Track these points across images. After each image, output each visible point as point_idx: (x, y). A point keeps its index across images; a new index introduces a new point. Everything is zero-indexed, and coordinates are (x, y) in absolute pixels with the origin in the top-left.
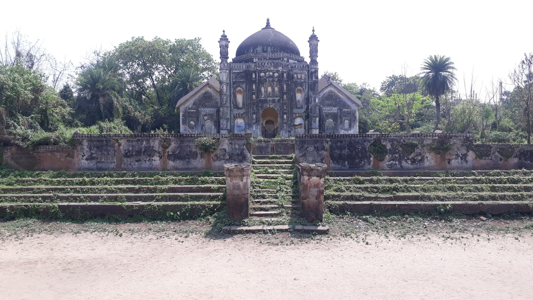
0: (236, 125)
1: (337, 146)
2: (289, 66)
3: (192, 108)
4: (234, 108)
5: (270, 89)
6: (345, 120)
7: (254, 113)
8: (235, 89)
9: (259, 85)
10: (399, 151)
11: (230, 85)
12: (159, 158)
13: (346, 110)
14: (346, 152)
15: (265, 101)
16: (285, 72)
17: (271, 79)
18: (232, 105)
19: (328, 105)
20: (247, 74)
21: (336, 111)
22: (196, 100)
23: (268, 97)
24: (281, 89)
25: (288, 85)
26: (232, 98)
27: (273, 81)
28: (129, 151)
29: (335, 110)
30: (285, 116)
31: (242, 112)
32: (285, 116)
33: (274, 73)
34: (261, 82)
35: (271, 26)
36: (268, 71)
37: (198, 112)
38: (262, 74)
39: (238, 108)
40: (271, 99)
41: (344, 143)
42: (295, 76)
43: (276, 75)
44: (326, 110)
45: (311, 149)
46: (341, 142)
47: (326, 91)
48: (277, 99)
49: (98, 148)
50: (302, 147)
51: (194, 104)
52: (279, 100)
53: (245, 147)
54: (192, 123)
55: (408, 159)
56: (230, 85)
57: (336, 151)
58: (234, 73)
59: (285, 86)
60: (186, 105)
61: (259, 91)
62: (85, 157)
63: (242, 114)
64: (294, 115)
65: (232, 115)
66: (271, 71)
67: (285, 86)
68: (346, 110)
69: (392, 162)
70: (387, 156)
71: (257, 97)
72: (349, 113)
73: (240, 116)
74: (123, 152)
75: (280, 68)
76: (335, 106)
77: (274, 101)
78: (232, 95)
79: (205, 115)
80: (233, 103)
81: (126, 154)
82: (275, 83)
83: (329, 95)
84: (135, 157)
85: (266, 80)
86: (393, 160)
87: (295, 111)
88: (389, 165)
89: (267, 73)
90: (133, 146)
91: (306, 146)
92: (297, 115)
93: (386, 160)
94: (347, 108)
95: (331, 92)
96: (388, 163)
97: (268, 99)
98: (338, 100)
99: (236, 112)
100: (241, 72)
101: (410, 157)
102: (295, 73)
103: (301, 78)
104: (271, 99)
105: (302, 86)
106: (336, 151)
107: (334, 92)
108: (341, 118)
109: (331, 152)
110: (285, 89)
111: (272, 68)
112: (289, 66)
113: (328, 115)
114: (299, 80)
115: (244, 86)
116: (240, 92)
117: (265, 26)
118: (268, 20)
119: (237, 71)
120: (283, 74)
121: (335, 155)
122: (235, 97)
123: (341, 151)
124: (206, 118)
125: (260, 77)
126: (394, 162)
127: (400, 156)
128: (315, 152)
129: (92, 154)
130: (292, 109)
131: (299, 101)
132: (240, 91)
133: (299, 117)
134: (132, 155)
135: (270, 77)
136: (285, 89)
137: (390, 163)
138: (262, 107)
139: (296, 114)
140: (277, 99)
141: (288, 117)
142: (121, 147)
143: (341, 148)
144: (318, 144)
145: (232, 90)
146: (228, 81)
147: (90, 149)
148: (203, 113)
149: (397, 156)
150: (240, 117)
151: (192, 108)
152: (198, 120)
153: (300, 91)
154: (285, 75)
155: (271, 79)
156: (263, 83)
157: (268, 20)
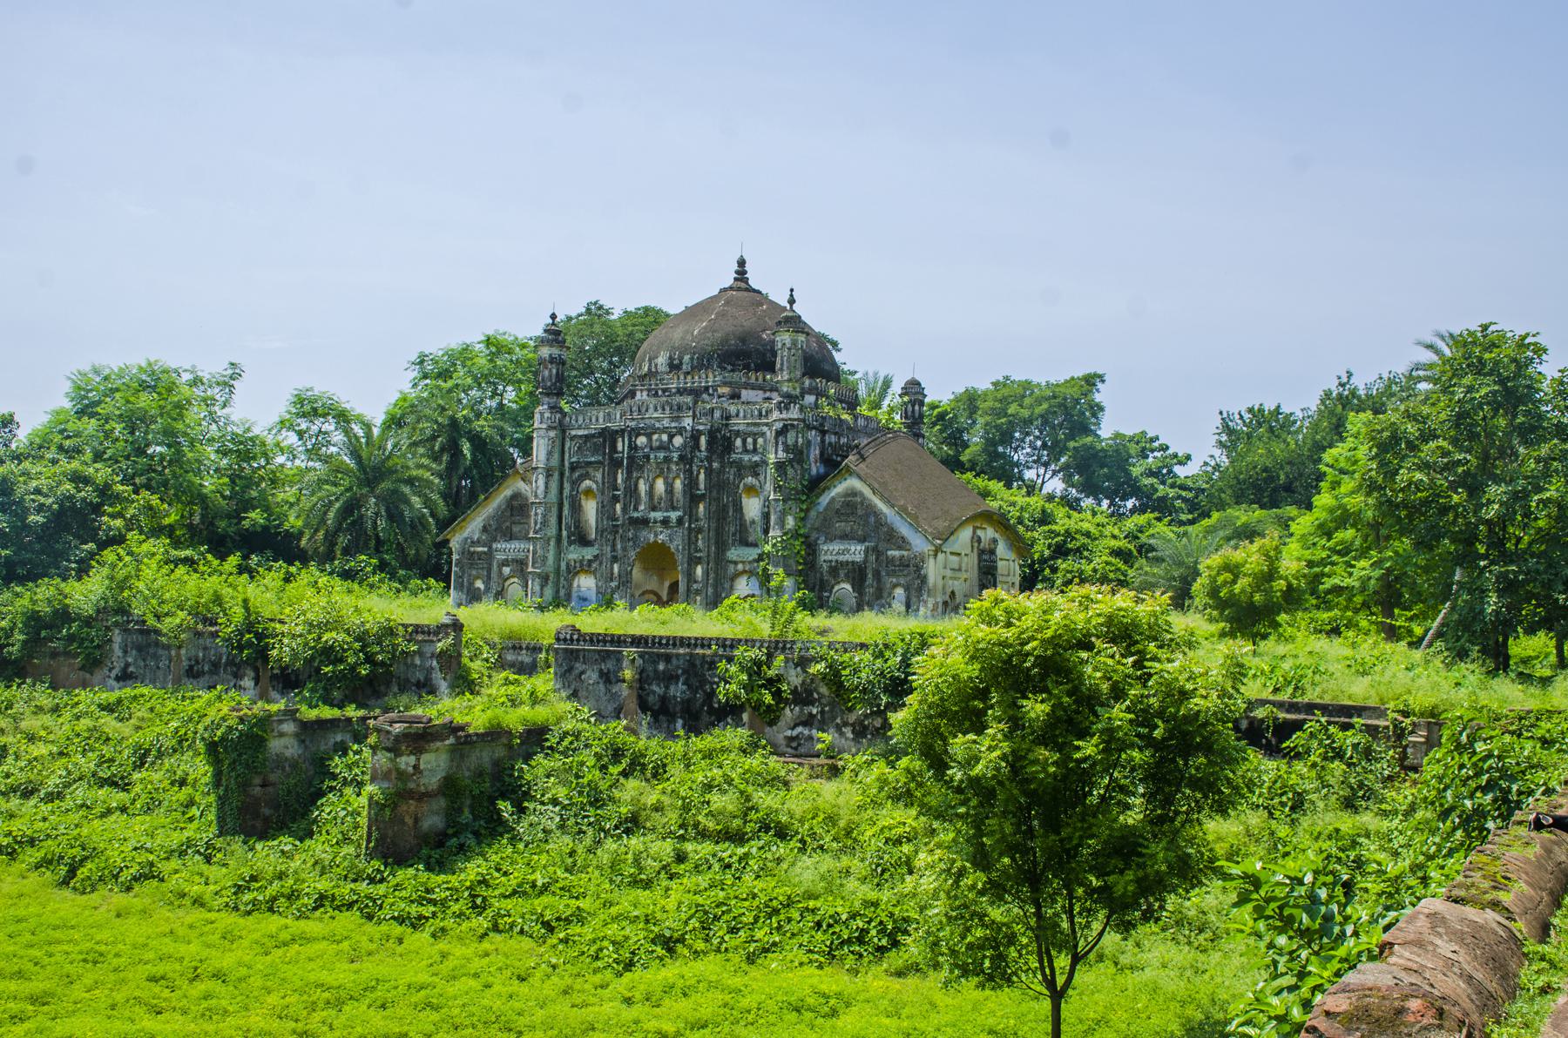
0: (574, 595)
1: (656, 671)
2: (717, 414)
3: (478, 543)
4: (570, 543)
5: (660, 485)
6: (895, 586)
7: (615, 559)
8: (575, 483)
9: (629, 472)
10: (821, 696)
11: (562, 475)
12: (252, 683)
13: (896, 553)
14: (678, 690)
15: (645, 522)
16: (700, 433)
17: (661, 455)
18: (564, 533)
19: (844, 537)
20: (609, 436)
21: (859, 558)
22: (489, 518)
23: (654, 509)
24: (691, 483)
25: (709, 472)
26: (566, 512)
27: (667, 460)
28: (197, 662)
29: (856, 552)
30: (699, 570)
31: (588, 553)
32: (699, 570)
33: (671, 437)
34: (636, 463)
35: (753, 283)
36: (656, 431)
37: (489, 555)
38: (642, 440)
39: (584, 541)
40: (658, 515)
41: (674, 661)
42: (738, 442)
43: (678, 441)
44: (831, 551)
45: (592, 676)
46: (668, 658)
47: (839, 488)
48: (674, 515)
49: (140, 649)
50: (570, 670)
51: (485, 529)
52: (680, 521)
53: (435, 663)
54: (479, 584)
55: (845, 724)
56: (562, 475)
57: (655, 688)
58: (572, 438)
59: (702, 476)
60: (465, 535)
61: (632, 491)
62: (113, 674)
63: (590, 561)
64: (731, 568)
65: (563, 565)
66: (664, 430)
67: (702, 476)
68: (896, 553)
69: (800, 729)
70: (787, 711)
71: (624, 510)
72: (904, 564)
73: (585, 567)
74: (185, 663)
75: (687, 422)
76: (862, 540)
77: (665, 522)
78: (566, 503)
79: (505, 563)
80: (568, 528)
81: (191, 667)
82: (674, 467)
83: (847, 504)
84: (207, 677)
85: (647, 457)
86: (804, 724)
87: (733, 554)
88: (791, 739)
89: (655, 437)
90: (205, 649)
91: (579, 666)
92: (740, 567)
93: (781, 723)
94: (900, 548)
95: (853, 493)
96: (789, 733)
97: (653, 515)
98: (872, 519)
99: (574, 554)
100: (593, 436)
101: (852, 718)
102: (738, 433)
103: (755, 450)
104: (658, 515)
105: (756, 475)
106: (655, 688)
107: (862, 494)
108: (877, 574)
109: (641, 688)
110: (702, 486)
111: (666, 423)
112: (717, 414)
113: (835, 569)
114: (746, 458)
115: (599, 476)
116: (588, 492)
117: (728, 280)
118: (742, 263)
119: (580, 433)
120: (695, 436)
121: (651, 699)
122: (576, 508)
123: (667, 688)
124: (506, 570)
125: (633, 447)
126: (806, 732)
127: (822, 712)
128: (601, 686)
129: (127, 665)
130: (722, 546)
131: (753, 522)
132: (588, 492)
133: (744, 572)
134: (203, 673)
135: (662, 447)
136: (702, 486)
137: (795, 733)
138: (635, 539)
139: (736, 563)
140: (674, 515)
141: (706, 573)
142: (183, 651)
143: (669, 678)
144: (609, 665)
145: (567, 486)
146: (555, 462)
147: (125, 652)
148: (500, 556)
149: (814, 711)
150: (582, 570)
151: (478, 543)
152: (489, 577)
153: (751, 490)
154: (703, 440)
155: (661, 455)
156: (641, 468)
157: (742, 263)
